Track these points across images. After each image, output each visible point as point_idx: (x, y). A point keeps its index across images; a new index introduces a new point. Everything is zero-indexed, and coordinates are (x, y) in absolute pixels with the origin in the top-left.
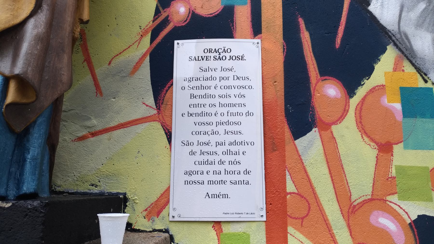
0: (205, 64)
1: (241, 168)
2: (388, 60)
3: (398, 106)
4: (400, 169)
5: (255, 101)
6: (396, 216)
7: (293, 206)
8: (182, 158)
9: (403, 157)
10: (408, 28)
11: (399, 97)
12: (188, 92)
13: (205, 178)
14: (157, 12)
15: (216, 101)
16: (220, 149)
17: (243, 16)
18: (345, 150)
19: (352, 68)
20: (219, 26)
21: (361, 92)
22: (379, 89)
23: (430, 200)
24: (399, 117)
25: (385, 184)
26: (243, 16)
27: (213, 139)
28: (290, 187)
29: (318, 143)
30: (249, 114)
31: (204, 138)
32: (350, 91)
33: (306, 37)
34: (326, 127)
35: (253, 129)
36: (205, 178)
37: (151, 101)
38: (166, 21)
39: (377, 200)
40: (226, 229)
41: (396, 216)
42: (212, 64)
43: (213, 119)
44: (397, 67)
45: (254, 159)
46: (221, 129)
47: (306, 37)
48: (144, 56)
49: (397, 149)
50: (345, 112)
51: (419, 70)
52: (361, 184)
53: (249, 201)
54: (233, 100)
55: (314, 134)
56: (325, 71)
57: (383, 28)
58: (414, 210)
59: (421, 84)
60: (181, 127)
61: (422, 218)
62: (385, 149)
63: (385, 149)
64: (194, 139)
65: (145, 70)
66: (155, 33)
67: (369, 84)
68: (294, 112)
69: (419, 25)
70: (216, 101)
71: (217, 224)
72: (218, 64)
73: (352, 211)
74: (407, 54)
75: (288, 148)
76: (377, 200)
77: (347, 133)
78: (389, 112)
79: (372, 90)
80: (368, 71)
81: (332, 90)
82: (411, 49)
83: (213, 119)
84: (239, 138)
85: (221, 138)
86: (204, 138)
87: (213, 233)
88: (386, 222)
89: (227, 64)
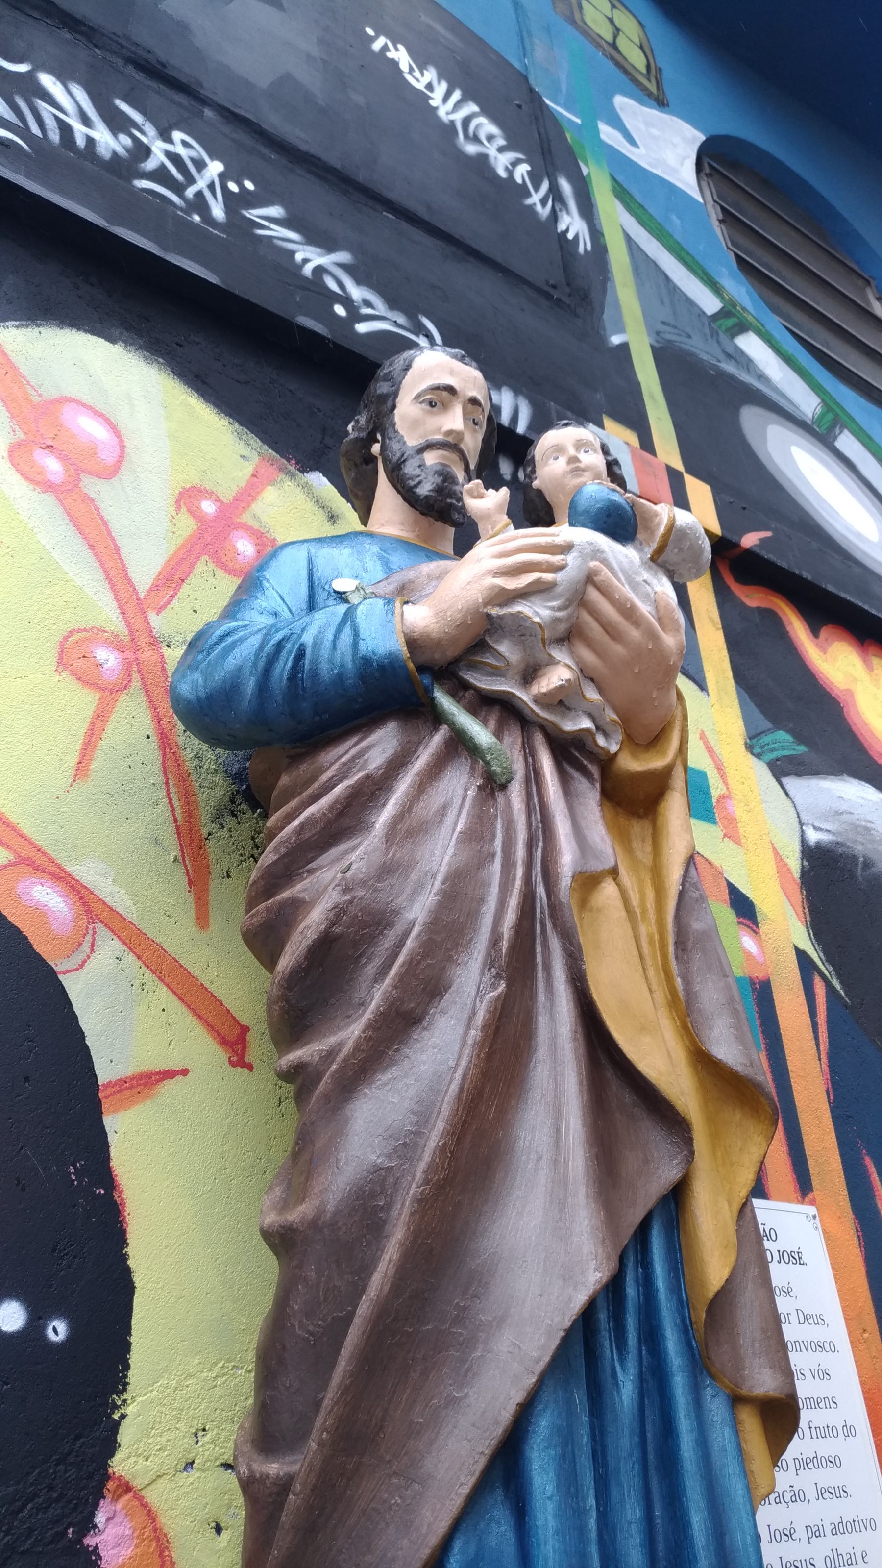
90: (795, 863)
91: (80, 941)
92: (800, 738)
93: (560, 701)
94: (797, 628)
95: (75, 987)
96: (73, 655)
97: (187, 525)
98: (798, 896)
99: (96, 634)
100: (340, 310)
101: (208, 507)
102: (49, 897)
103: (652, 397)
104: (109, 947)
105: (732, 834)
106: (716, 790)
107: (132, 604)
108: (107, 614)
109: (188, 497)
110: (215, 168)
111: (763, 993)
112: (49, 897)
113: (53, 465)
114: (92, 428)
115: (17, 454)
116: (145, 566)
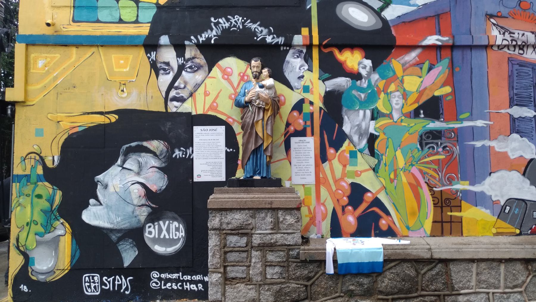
0: (299, 144)
1: (309, 171)
2: (347, 142)
3: (348, 155)
4: (348, 171)
5: (312, 154)
6: (346, 182)
7: (322, 180)
8: (294, 169)
9: (349, 168)
10: (352, 134)
11: (349, 153)
12: (295, 152)
13: (300, 174)
14: (285, 129)
15: (302, 154)
16: (304, 167)
17: (309, 130)
18: (335, 166)
19: (337, 145)
20: (302, 133)
21: (339, 152)
22: (344, 151)
23: (354, 178)
24: (349, 158)
25: (344, 175)
26: (309, 130)
27: (302, 164)
28: (321, 176)
29: (328, 165)
30: (311, 158)
31: (300, 164)
32: (337, 151)
33: (326, 136)
34: (330, 161)
35: (312, 161)
36: (300, 174)
37: (285, 154)
38: (288, 132)
39: (342, 179)
40: (305, 186)
41: (346, 182)
42: (301, 144)
43: (302, 159)
44: (349, 145)
45: (312, 169)
46: (304, 161)
47: (326, 136)
48: (282, 142)
49: (348, 166)
50: (335, 157)
51: (354, 146)
52: (338, 175)
53: (311, 179)
54: (307, 154)
55: (327, 163)
56: (331, 146)
57: (346, 134)
58: (350, 181)
59: (354, 149)
60: (293, 161)
61: (352, 183)
62: (345, 166)
63: (345, 166)
64: (297, 164)
65: (283, 145)
66: (285, 135)
67: (341, 149)
68: (322, 157)
69: (355, 133)
70: (302, 154)
71: (303, 185)
72: (303, 144)
73: (336, 181)
74: (352, 141)
75: (321, 166)
76: (342, 179)
77: (336, 162)
78: (346, 157)
79: (342, 151)
80: (341, 146)
81: (331, 151)
82: (352, 140)
83: (302, 159)
84: (308, 164)
85: (304, 164)
86: (300, 164)
87: (303, 187)
88: (344, 184)
89: (305, 144)
90: (323, 95)
91: (233, 123)
92: (330, 74)
93: (259, 104)
94: (336, 52)
95: (233, 127)
96: (230, 97)
97: (240, 77)
98: (322, 99)
99: (232, 94)
100: (255, 38)
101: (242, 74)
102: (230, 120)
103: (314, 16)
104: (236, 123)
105: (312, 94)
106: (311, 87)
107: (235, 90)
108: (233, 92)
109: (239, 74)
110: (241, 18)
111: (312, 114)
112: (230, 120)
113: (226, 76)
114: (229, 70)
115: (223, 77)
116: (235, 85)
